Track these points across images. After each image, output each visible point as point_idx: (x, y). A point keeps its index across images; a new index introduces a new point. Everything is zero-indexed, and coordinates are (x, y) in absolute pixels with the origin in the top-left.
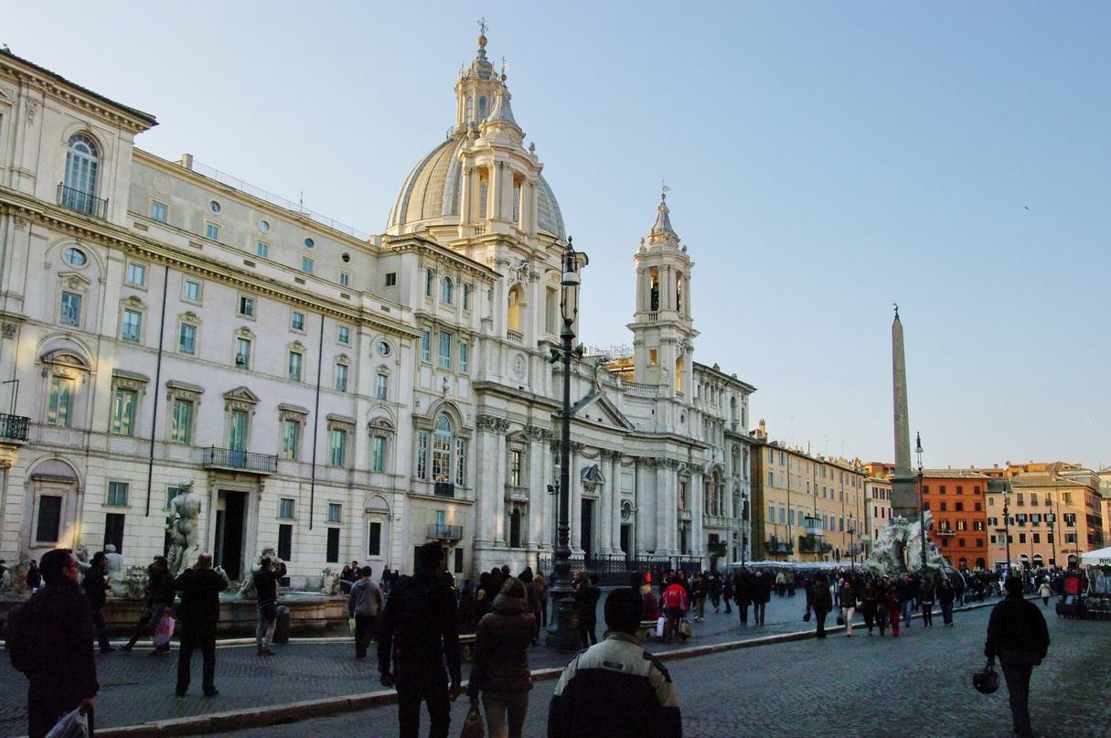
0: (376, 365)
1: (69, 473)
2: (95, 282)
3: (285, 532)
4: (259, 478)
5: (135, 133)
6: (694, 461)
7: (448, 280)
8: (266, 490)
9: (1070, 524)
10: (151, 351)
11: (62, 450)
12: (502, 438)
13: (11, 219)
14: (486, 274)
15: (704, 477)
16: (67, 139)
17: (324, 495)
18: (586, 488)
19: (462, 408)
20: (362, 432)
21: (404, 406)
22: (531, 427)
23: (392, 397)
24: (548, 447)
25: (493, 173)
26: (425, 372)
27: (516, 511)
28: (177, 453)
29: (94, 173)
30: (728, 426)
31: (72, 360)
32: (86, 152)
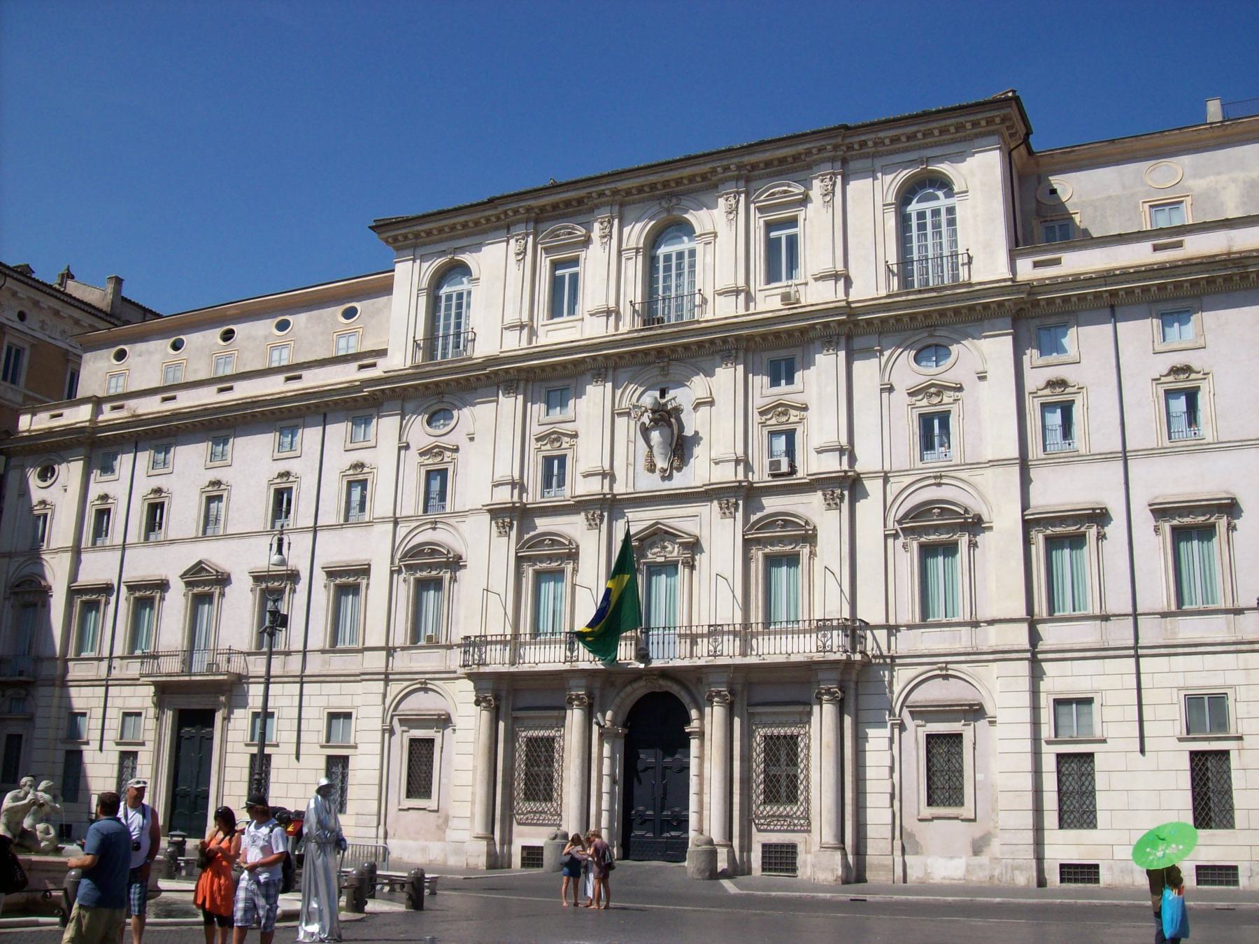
10: (1106, 457)
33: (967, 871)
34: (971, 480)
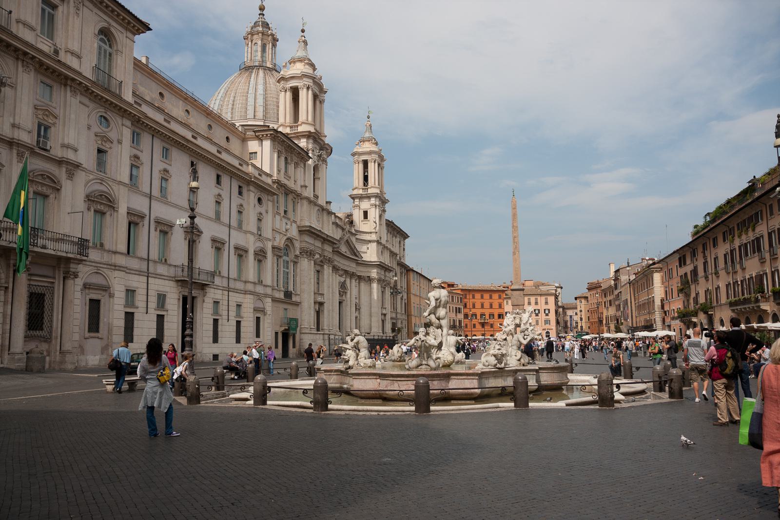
0: (256, 212)
1: (104, 283)
2: (115, 142)
3: (216, 321)
4: (203, 287)
5: (134, 34)
6: (387, 279)
7: (286, 158)
8: (208, 295)
9: (547, 315)
10: (144, 194)
11: (101, 266)
12: (313, 262)
13: (68, 88)
14: (302, 156)
15: (391, 288)
16: (97, 33)
17: (235, 298)
18: (340, 294)
19: (295, 242)
20: (251, 256)
21: (270, 240)
22: (324, 256)
23: (264, 234)
24: (331, 268)
25: (303, 94)
26: (278, 217)
27: (319, 308)
28: (161, 269)
29: (110, 60)
30: (398, 258)
31: (105, 199)
32: (106, 45)
33: (100, 361)
34: (112, 187)
